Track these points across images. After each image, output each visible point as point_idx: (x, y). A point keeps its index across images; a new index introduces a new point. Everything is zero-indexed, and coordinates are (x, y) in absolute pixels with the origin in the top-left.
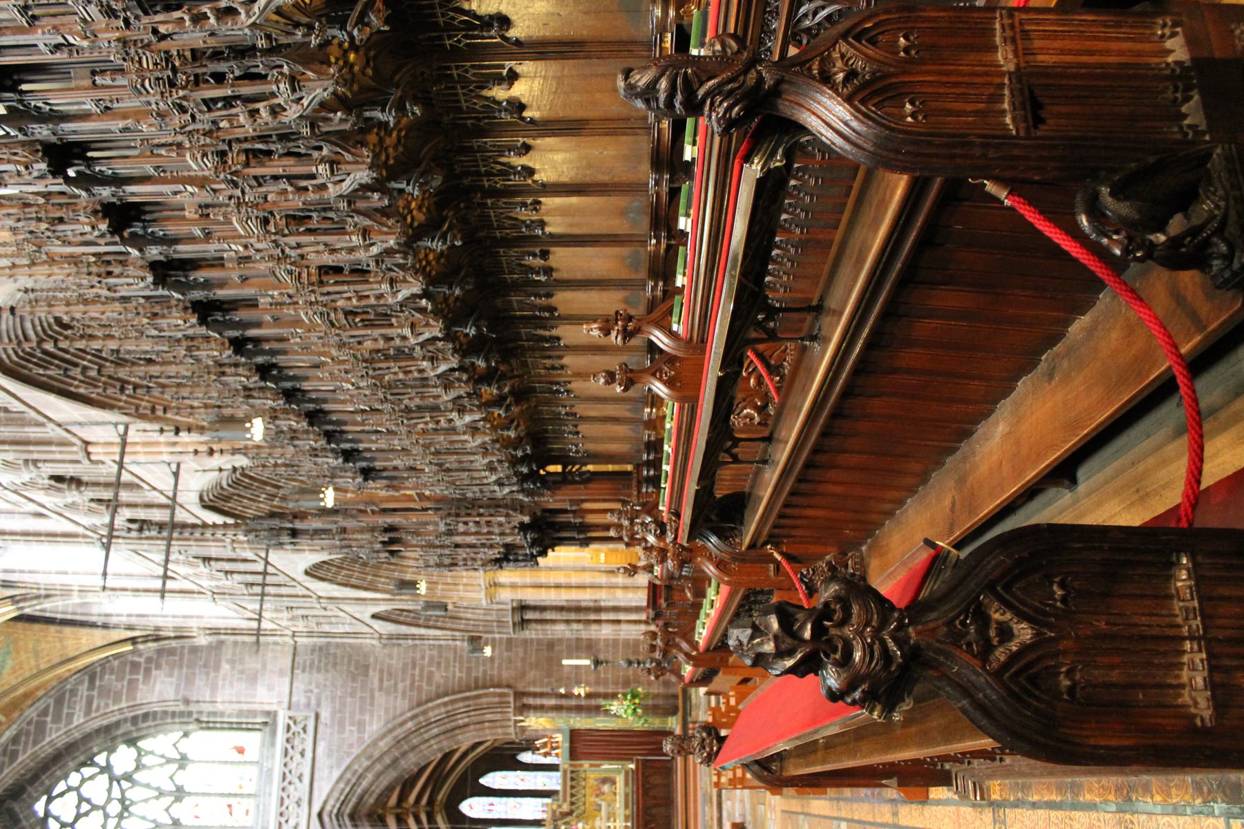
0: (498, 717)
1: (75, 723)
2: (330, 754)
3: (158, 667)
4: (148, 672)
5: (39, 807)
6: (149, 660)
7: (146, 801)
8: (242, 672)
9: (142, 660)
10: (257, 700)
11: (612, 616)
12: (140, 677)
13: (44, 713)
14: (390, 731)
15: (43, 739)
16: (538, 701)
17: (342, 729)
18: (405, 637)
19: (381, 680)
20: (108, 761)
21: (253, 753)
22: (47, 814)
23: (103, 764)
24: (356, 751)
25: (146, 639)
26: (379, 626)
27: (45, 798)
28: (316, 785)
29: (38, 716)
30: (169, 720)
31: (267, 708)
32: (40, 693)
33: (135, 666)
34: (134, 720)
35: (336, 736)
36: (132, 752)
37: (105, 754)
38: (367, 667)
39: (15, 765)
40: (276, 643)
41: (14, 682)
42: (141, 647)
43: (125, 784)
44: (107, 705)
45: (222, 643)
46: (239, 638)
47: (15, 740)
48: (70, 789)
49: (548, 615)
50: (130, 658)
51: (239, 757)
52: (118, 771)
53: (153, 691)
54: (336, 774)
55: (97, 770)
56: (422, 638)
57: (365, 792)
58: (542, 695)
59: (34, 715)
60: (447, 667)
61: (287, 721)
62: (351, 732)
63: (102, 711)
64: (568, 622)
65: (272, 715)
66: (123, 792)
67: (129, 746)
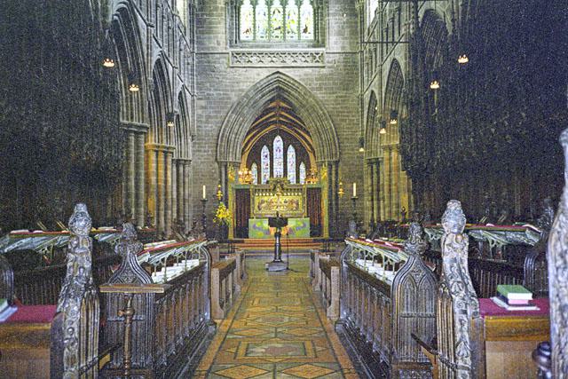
0: (326, 153)
8: (343, 28)
11: (375, 206)
14: (317, 102)
16: (333, 172)
18: (362, 107)
19: (341, 97)
26: (368, 94)
28: (291, 69)
31: (327, 42)
38: (347, 90)
45: (356, 16)
46: (359, 24)
49: (375, 175)
51: (302, 29)
54: (296, 79)
56: (362, 115)
57: (290, 93)
58: (337, 174)
60: (348, 128)
62: (316, 84)
64: (372, 185)
65: (323, 45)
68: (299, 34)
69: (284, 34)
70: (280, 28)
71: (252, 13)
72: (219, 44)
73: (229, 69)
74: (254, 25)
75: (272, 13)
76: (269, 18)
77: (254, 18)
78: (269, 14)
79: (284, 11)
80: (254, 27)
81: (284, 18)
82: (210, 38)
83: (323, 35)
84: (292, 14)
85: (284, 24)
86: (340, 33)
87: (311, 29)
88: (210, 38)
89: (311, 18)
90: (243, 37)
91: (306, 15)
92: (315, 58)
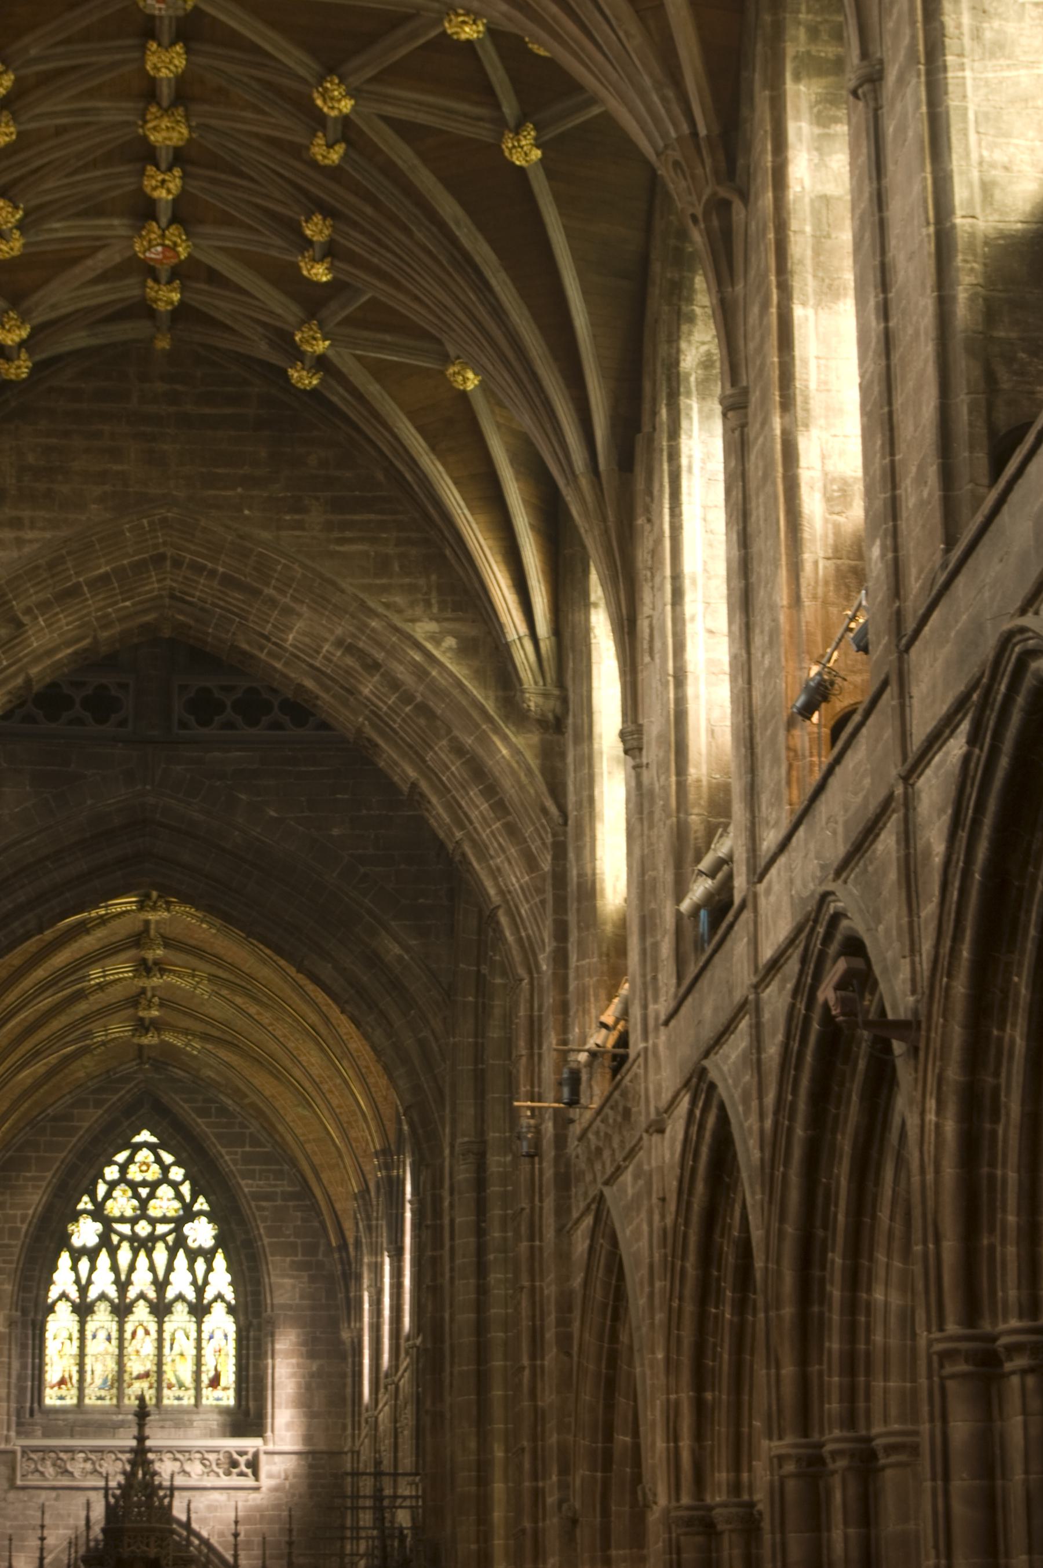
1: (243, 1183)
3: (312, 1279)
5: (145, 1136)
7: (152, 1268)
9: (320, 1257)
10: (277, 1411)
12: (299, 1258)
15: (224, 1146)
20: (201, 1213)
23: (196, 1207)
27: (153, 1140)
29: (251, 1134)
30: (249, 1288)
32: (277, 1137)
33: (311, 1249)
36: (208, 1243)
37: (206, 1207)
39: (194, 1115)
40: (344, 1428)
41: (288, 1119)
42: (336, 1256)
43: (170, 1239)
44: (264, 1219)
45: (344, 1358)
46: (349, 1380)
48: (165, 1169)
50: (323, 1241)
52: (187, 1229)
53: (283, 1276)
55: (188, 1199)
59: (252, 1130)
61: (251, 1451)
63: (257, 1213)
66: (163, 1238)
67: (215, 1237)
68: (198, 1389)
69: (159, 1390)
70: (147, 1375)
71: (76, 1335)
74: (81, 1365)
75: (128, 1335)
76: (121, 1347)
77: (82, 1347)
78: (121, 1339)
79: (160, 1331)
80: (81, 1372)
81: (160, 1347)
84: (180, 1336)
85: (160, 1364)
87: (229, 1378)
89: (231, 1347)
90: (51, 1398)
91: (218, 1341)
92: (234, 1464)
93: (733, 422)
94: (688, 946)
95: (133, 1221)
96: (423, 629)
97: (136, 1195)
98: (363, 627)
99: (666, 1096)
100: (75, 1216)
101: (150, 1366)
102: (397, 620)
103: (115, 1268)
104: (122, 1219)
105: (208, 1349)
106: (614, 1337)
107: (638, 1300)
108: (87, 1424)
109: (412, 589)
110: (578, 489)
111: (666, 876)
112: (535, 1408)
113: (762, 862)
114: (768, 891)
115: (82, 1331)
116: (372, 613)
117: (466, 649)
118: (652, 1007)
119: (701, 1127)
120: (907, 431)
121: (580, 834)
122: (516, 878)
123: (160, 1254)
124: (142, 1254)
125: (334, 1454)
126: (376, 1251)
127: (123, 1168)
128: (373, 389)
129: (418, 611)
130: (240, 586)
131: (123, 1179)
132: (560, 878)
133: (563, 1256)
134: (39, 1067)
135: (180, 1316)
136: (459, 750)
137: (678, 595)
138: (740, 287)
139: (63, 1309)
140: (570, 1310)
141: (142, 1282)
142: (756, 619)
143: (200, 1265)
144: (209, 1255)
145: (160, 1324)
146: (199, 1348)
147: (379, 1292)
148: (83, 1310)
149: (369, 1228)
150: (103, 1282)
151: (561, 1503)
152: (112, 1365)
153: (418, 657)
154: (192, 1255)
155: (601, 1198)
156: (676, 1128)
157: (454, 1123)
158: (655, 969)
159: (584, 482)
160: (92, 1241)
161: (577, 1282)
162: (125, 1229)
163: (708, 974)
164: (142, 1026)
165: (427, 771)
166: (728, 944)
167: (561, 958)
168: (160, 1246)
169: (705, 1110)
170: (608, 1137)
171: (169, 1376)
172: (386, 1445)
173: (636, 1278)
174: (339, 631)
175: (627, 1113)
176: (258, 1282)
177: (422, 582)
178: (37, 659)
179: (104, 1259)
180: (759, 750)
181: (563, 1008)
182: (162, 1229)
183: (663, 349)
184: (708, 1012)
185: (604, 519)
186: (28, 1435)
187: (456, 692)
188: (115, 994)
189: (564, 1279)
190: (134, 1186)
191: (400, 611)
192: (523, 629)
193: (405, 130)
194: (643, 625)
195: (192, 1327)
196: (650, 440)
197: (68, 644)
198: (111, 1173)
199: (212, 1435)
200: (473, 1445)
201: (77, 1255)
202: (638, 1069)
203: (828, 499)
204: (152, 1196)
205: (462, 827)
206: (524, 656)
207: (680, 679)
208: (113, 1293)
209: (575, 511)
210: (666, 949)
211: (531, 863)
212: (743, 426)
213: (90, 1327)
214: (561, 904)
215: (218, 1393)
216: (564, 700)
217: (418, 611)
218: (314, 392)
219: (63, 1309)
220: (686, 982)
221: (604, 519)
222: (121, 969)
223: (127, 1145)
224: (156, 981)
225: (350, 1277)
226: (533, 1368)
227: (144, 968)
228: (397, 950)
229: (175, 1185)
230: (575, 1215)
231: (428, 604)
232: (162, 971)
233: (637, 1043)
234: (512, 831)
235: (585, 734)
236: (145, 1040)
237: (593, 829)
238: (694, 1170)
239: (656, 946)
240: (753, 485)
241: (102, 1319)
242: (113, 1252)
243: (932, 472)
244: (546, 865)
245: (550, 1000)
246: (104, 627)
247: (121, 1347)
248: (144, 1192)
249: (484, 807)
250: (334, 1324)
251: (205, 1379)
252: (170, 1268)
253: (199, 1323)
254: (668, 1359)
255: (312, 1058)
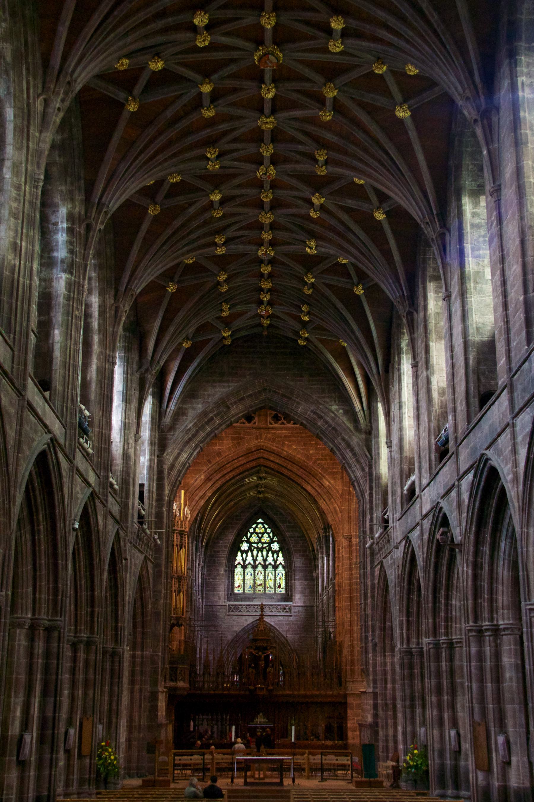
2: (279, 621)
3: (305, 559)
4: (303, 556)
5: (260, 520)
6: (307, 556)
13: (290, 523)
17: (286, 624)
20: (275, 541)
21: (278, 591)
22: (258, 523)
24: (280, 630)
25: (314, 555)
33: (305, 551)
34: (288, 549)
35: (284, 623)
36: (278, 549)
45: (314, 580)
47: (281, 514)
48: (266, 529)
51: (277, 586)
54: (272, 624)
62: (286, 628)
66: (265, 548)
68: (275, 589)
69: (265, 589)
70: (261, 585)
72: (220, 598)
73: (226, 617)
74: (244, 582)
76: (254, 577)
77: (244, 577)
78: (254, 575)
79: (265, 573)
80: (244, 584)
81: (265, 577)
82: (214, 595)
83: (291, 591)
85: (265, 582)
86: (302, 593)
87: (283, 585)
88: (214, 595)
90: (236, 591)
92: (285, 609)
93: (415, 370)
94: (404, 500)
95: (257, 543)
96: (334, 407)
97: (258, 536)
98: (318, 408)
99: (399, 541)
100: (242, 542)
101: (262, 582)
102: (327, 406)
103: (253, 556)
104: (254, 543)
105: (278, 578)
106: (386, 597)
107: (392, 591)
108: (245, 598)
109: (331, 397)
110: (374, 378)
111: (398, 481)
112: (365, 614)
113: (423, 487)
114: (424, 495)
115: (244, 573)
116: (320, 404)
117: (346, 413)
118: (395, 516)
119: (408, 550)
120: (458, 390)
121: (375, 463)
122: (359, 473)
123: (265, 553)
124: (260, 553)
125: (312, 607)
126: (322, 553)
127: (255, 529)
128: (320, 346)
129: (333, 403)
130: (286, 397)
131: (254, 532)
132: (370, 474)
133: (372, 574)
134: (232, 503)
135: (270, 569)
136: (343, 439)
137: (400, 407)
138: (416, 335)
139: (239, 566)
140: (374, 588)
141: (260, 559)
142: (421, 423)
143: (275, 555)
144: (278, 553)
145: (265, 571)
146: (275, 577)
147: (323, 564)
148: (244, 567)
149: (320, 547)
150: (249, 559)
151: (372, 640)
152: (252, 582)
153: (333, 415)
154: (273, 553)
155: (382, 562)
156: (402, 548)
157: (343, 529)
158: (396, 505)
159: (376, 376)
160: (246, 548)
161: (376, 581)
162: (255, 545)
163: (409, 511)
164: (259, 492)
165: (335, 445)
166: (414, 505)
167: (371, 495)
168: (265, 550)
169: (409, 546)
170: (384, 545)
171: (267, 585)
172: (325, 606)
173: (391, 585)
174: (312, 408)
175: (389, 541)
176: (290, 560)
177: (333, 395)
178: (234, 416)
179: (250, 554)
180: (422, 457)
181: (371, 508)
182: (265, 545)
183: (396, 341)
184: (409, 521)
185: (381, 385)
186: (230, 601)
187: (343, 424)
188: (252, 485)
189: (373, 580)
190: (257, 534)
191: (327, 403)
192: (360, 408)
193: (329, 286)
194: (392, 414)
195: (273, 572)
196: (393, 365)
197: (241, 412)
198: (251, 530)
199: (279, 601)
200: (349, 616)
201: (242, 552)
202: (391, 530)
203: (439, 393)
204: (262, 536)
205: (345, 460)
206: (360, 415)
207: (401, 429)
208: (252, 562)
209: (373, 383)
210: (398, 500)
211: (363, 470)
212: (417, 371)
213: (246, 572)
214: (371, 480)
215: (280, 590)
216: (371, 427)
217: (333, 403)
218: (305, 346)
219: (239, 567)
220: (404, 511)
221: (381, 385)
222: (254, 479)
223: (255, 523)
224: (263, 482)
225: (315, 558)
226: (365, 604)
227: (260, 478)
228: (328, 483)
229: (268, 534)
230: (376, 564)
231: (335, 401)
232: (265, 479)
233: (391, 524)
234: (358, 461)
235: (377, 436)
236: (260, 496)
237: (379, 462)
238: (406, 561)
239: (396, 499)
240: (420, 387)
241: (249, 570)
242: (252, 552)
243: (464, 403)
244: (367, 470)
245: (368, 506)
246: (251, 407)
247: (254, 577)
248: (260, 535)
249: (350, 454)
250: (311, 572)
251: (277, 586)
252: (267, 556)
253: (275, 571)
254: (400, 609)
255: (305, 502)
